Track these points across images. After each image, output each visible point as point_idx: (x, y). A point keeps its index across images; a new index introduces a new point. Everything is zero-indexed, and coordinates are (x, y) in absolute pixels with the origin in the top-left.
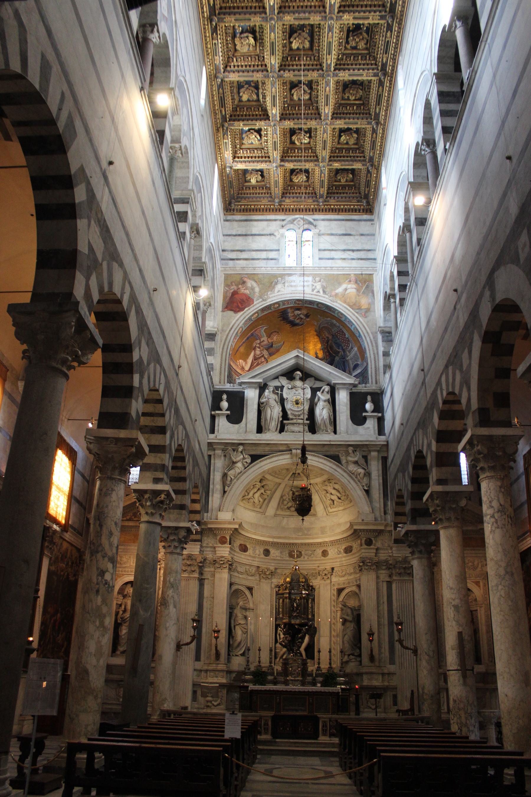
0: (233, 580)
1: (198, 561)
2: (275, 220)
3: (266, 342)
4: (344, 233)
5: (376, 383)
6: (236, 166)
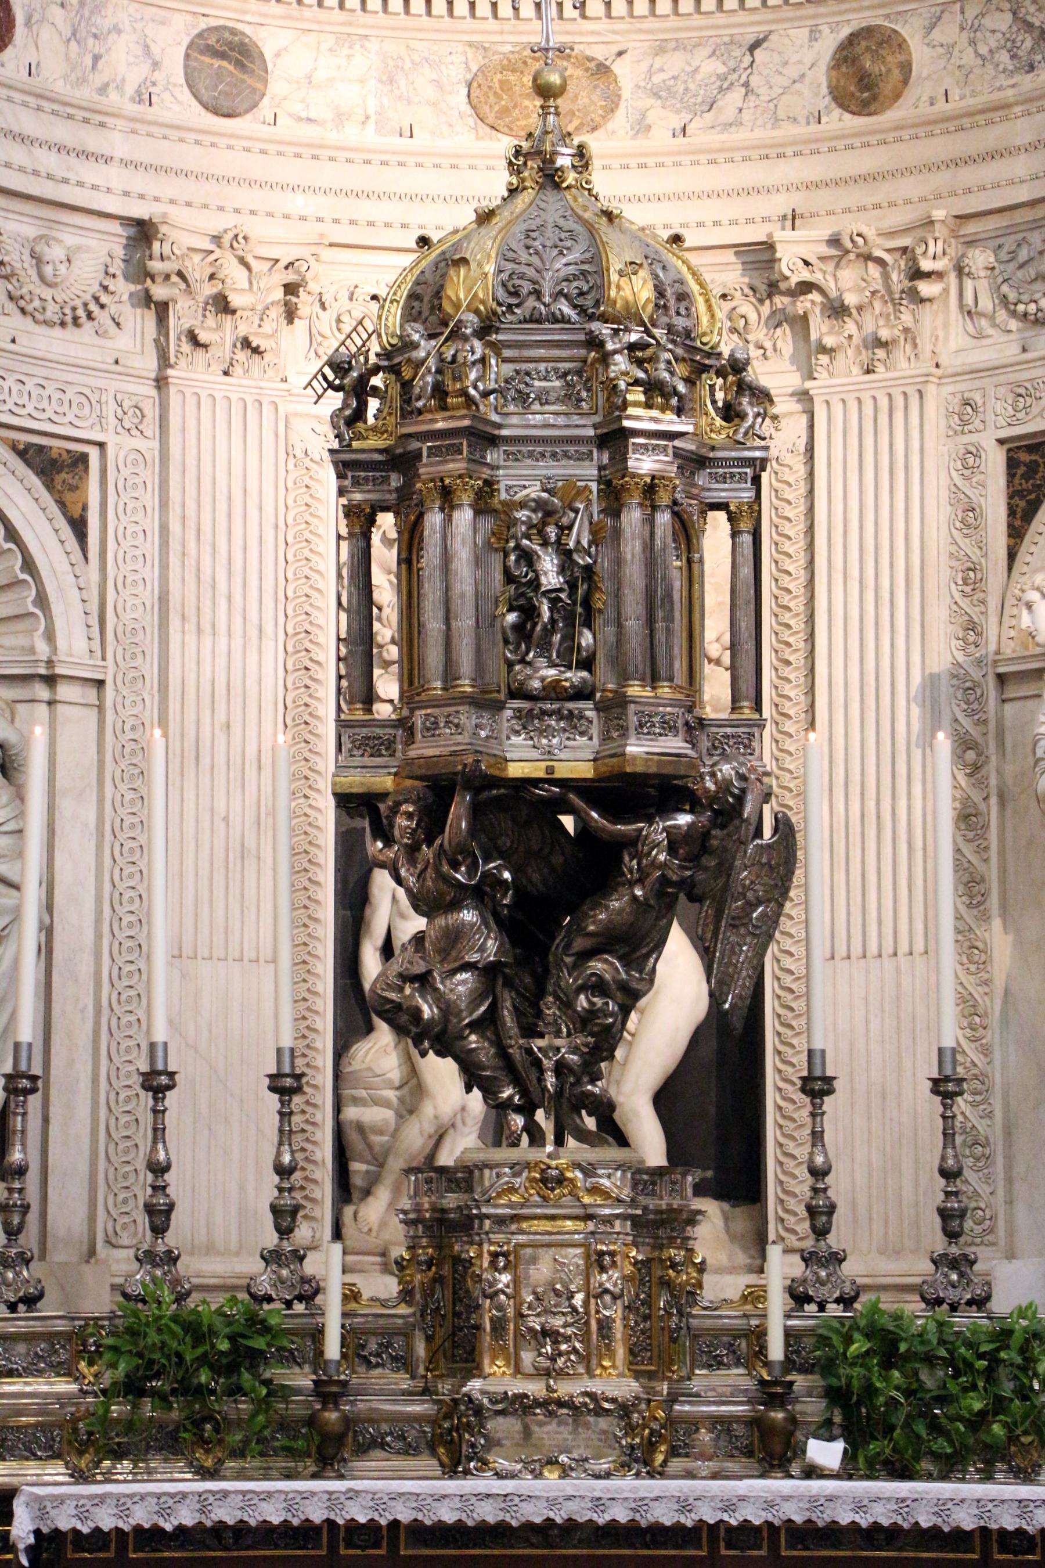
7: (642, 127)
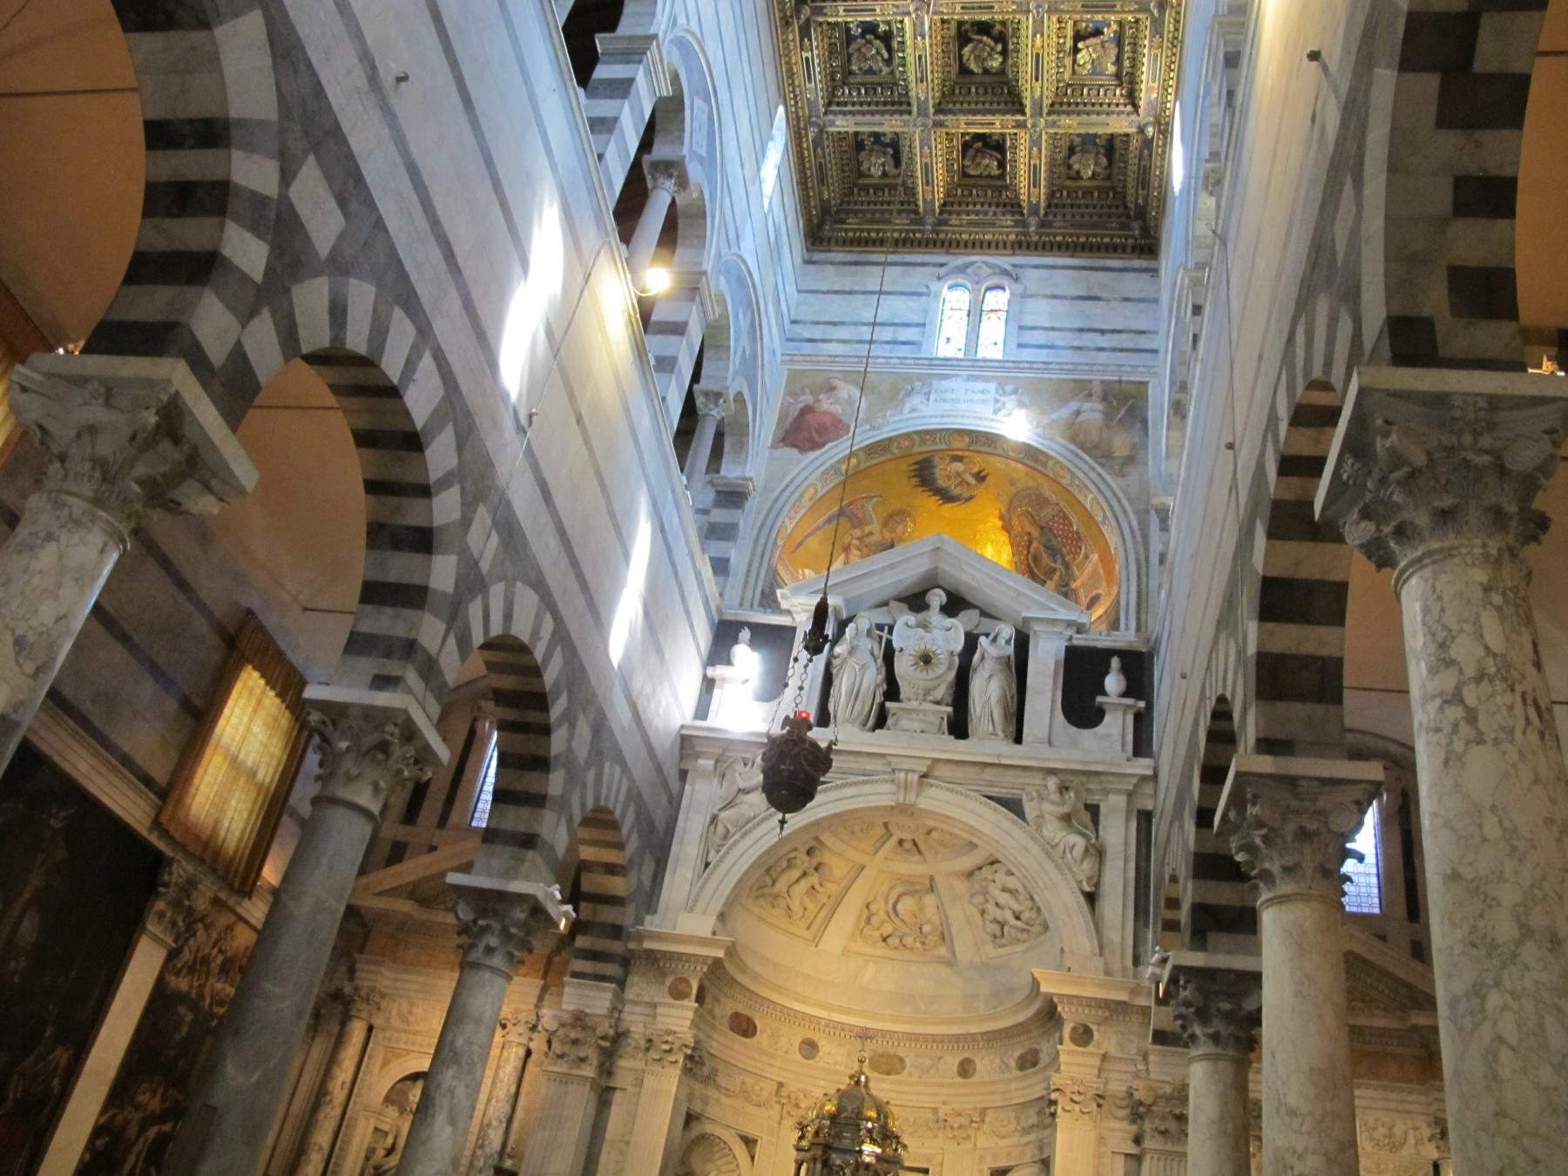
0: (697, 1107)
1: (599, 1033)
2: (923, 265)
3: (873, 539)
4: (1084, 293)
5: (1138, 629)
6: (833, 124)
7: (910, 1074)
